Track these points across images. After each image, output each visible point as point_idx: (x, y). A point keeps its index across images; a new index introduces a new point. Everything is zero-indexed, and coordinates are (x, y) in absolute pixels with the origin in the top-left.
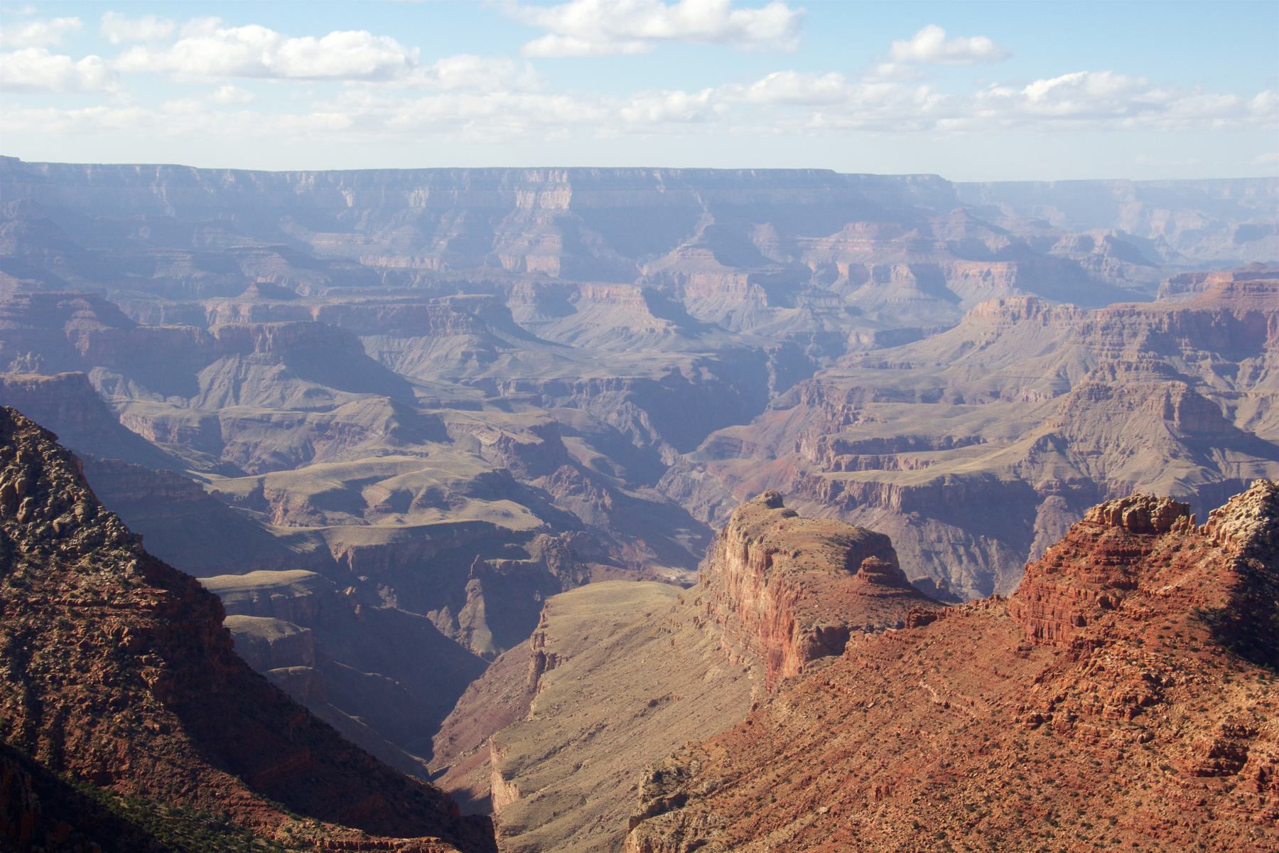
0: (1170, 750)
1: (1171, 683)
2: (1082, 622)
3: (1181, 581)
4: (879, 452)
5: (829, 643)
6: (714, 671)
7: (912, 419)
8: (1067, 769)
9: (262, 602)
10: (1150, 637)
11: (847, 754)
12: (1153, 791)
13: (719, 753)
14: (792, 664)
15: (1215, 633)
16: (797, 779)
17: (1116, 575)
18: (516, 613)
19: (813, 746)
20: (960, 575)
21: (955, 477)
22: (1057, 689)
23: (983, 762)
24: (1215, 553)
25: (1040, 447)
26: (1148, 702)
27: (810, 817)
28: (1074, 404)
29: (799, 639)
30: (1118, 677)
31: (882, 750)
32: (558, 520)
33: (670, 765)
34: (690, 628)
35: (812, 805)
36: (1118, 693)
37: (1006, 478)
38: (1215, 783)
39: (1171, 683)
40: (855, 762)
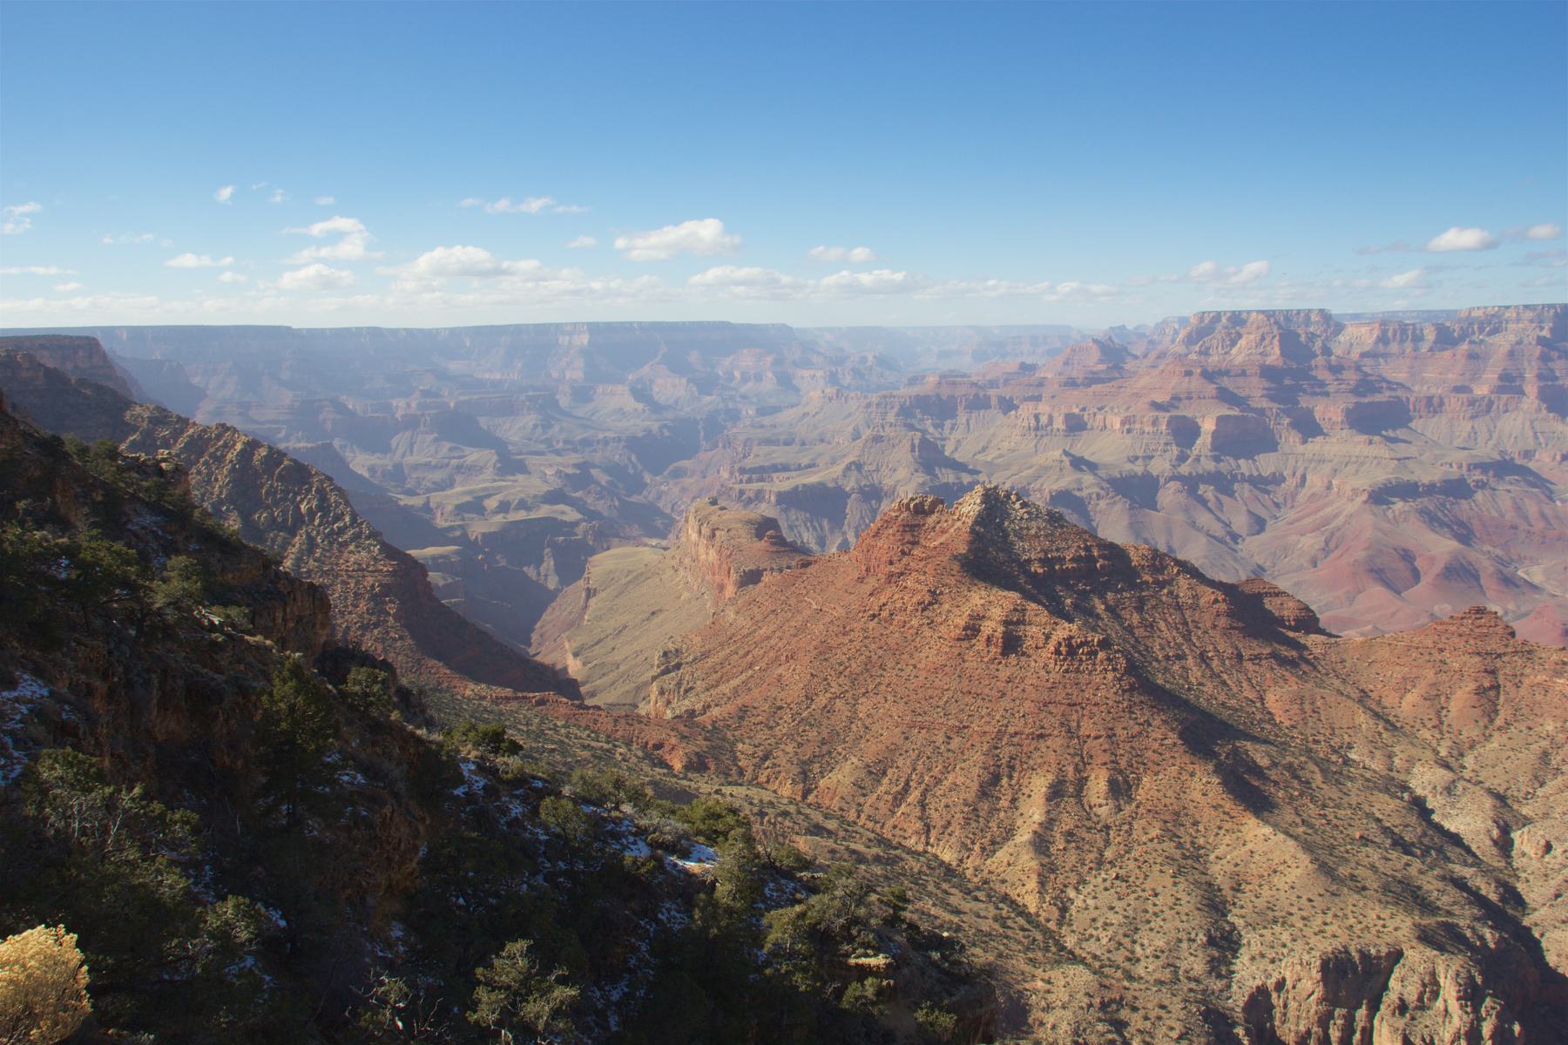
0: (943, 628)
2: (891, 563)
3: (942, 539)
4: (763, 472)
5: (751, 578)
6: (686, 595)
7: (780, 455)
8: (890, 641)
10: (930, 569)
11: (768, 638)
12: (934, 649)
14: (730, 590)
15: (962, 566)
16: (741, 652)
17: (908, 537)
18: (572, 564)
20: (808, 538)
22: (883, 600)
24: (959, 524)
25: (848, 468)
26: (930, 604)
29: (734, 576)
30: (915, 592)
32: (592, 515)
33: (671, 646)
34: (671, 572)
35: (751, 666)
36: (914, 600)
37: (831, 485)
38: (965, 644)
40: (772, 642)
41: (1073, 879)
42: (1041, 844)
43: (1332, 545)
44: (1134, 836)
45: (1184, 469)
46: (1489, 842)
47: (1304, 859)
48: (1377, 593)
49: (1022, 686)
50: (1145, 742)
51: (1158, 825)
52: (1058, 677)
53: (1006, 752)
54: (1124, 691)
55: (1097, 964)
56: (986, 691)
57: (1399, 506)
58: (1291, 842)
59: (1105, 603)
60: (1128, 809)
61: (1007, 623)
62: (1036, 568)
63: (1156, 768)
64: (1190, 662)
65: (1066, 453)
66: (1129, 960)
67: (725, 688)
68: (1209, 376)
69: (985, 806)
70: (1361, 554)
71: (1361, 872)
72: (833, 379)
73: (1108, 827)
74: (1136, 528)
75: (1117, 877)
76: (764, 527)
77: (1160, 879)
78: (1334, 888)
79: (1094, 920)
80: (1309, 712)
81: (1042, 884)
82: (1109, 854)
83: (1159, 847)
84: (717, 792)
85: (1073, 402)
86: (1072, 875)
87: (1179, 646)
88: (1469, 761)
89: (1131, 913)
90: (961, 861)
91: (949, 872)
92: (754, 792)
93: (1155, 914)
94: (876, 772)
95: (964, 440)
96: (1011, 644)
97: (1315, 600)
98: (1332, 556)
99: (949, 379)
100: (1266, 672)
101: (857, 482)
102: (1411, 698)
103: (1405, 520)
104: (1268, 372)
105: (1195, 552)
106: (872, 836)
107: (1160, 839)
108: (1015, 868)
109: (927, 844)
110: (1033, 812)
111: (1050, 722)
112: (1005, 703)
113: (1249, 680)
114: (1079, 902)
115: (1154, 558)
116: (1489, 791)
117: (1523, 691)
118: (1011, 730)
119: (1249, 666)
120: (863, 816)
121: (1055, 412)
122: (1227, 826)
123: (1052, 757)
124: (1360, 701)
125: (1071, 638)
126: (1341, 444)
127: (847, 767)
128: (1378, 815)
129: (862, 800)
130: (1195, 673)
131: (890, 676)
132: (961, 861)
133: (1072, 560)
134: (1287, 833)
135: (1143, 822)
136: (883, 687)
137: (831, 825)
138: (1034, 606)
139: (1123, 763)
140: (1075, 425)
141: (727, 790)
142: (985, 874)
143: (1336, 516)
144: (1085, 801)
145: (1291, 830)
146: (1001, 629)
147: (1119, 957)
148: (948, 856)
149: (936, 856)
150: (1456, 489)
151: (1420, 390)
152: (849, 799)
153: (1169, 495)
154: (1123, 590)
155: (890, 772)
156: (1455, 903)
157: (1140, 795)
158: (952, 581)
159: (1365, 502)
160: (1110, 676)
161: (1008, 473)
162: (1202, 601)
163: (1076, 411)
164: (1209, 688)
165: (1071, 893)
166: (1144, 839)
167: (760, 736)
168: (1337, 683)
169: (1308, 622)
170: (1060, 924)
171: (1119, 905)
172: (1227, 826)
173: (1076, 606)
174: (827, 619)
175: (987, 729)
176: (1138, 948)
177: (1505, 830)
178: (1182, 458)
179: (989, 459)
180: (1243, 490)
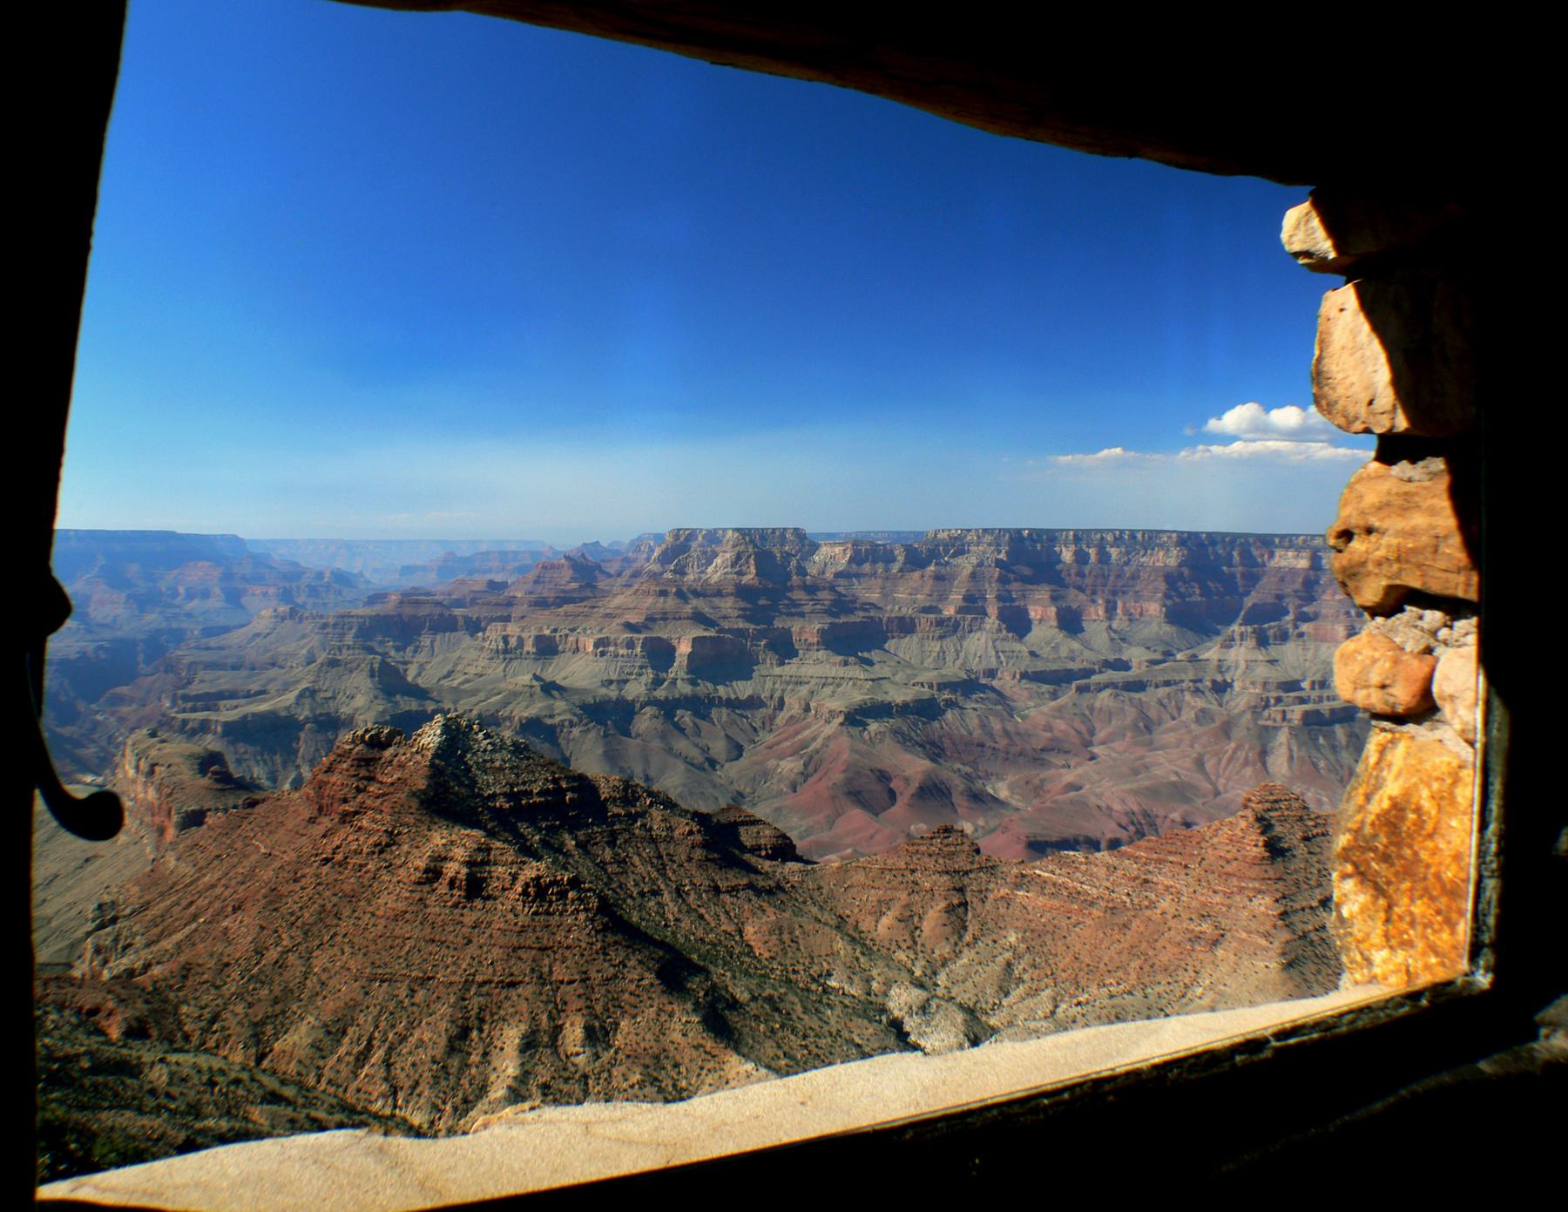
0: (401, 871)
1: (399, 833)
2: (345, 801)
4: (210, 701)
5: (194, 819)
7: (225, 680)
8: (345, 886)
10: (386, 808)
11: (213, 886)
12: (392, 895)
13: (136, 889)
14: (171, 833)
15: (422, 803)
16: (184, 903)
17: (363, 773)
19: (191, 883)
20: (259, 772)
21: (254, 714)
23: (297, 887)
25: (301, 695)
27: (194, 926)
28: (320, 670)
29: (175, 818)
30: (370, 833)
31: (233, 882)
33: (107, 898)
35: (195, 917)
36: (371, 841)
37: (284, 714)
38: (427, 888)
39: (399, 833)
40: (218, 890)
43: (811, 769)
44: (614, 1083)
45: (661, 693)
48: (856, 816)
49: (488, 932)
50: (622, 984)
51: (638, 1070)
52: (527, 920)
53: (475, 1003)
54: (597, 932)
56: (451, 938)
57: (874, 726)
59: (575, 838)
60: (606, 1056)
61: (470, 864)
62: (500, 803)
63: (634, 1011)
64: (666, 897)
65: (536, 677)
67: (167, 944)
69: (455, 1062)
70: (838, 777)
72: (286, 596)
73: (586, 1076)
74: (612, 757)
76: (208, 762)
80: (788, 942)
84: (162, 1060)
85: (544, 623)
87: (654, 881)
88: (942, 979)
90: (432, 1122)
92: (203, 1061)
94: (336, 1031)
95: (429, 665)
96: (475, 887)
97: (796, 828)
98: (810, 780)
99: (411, 598)
100: (743, 904)
101: (312, 710)
102: (885, 921)
104: (742, 592)
105: (672, 782)
106: (334, 1101)
107: (641, 1084)
109: (395, 1107)
111: (521, 968)
112: (472, 950)
113: (727, 913)
115: (625, 789)
116: (960, 1006)
117: (988, 905)
118: (479, 978)
119: (727, 898)
121: (524, 631)
123: (524, 1006)
124: (838, 928)
125: (538, 878)
126: (816, 665)
127: (303, 1028)
128: (857, 1040)
129: (321, 1063)
130: (672, 909)
131: (345, 926)
132: (432, 1122)
133: (540, 794)
134: (768, 1067)
136: (339, 939)
137: (289, 1092)
138: (499, 844)
139: (599, 1008)
140: (547, 648)
141: (173, 1058)
143: (814, 739)
144: (561, 1050)
145: (773, 1064)
146: (465, 870)
150: (926, 709)
151: (891, 611)
152: (308, 1062)
153: (645, 722)
154: (593, 824)
155: (350, 1030)
157: (619, 1040)
158: (410, 819)
159: (842, 724)
160: (582, 916)
161: (473, 700)
162: (677, 833)
163: (547, 632)
164: (686, 924)
166: (625, 1085)
167: (205, 999)
168: (815, 910)
169: (784, 850)
172: (711, 1065)
173: (544, 842)
174: (277, 864)
175: (453, 978)
178: (658, 682)
179: (455, 683)
180: (720, 715)
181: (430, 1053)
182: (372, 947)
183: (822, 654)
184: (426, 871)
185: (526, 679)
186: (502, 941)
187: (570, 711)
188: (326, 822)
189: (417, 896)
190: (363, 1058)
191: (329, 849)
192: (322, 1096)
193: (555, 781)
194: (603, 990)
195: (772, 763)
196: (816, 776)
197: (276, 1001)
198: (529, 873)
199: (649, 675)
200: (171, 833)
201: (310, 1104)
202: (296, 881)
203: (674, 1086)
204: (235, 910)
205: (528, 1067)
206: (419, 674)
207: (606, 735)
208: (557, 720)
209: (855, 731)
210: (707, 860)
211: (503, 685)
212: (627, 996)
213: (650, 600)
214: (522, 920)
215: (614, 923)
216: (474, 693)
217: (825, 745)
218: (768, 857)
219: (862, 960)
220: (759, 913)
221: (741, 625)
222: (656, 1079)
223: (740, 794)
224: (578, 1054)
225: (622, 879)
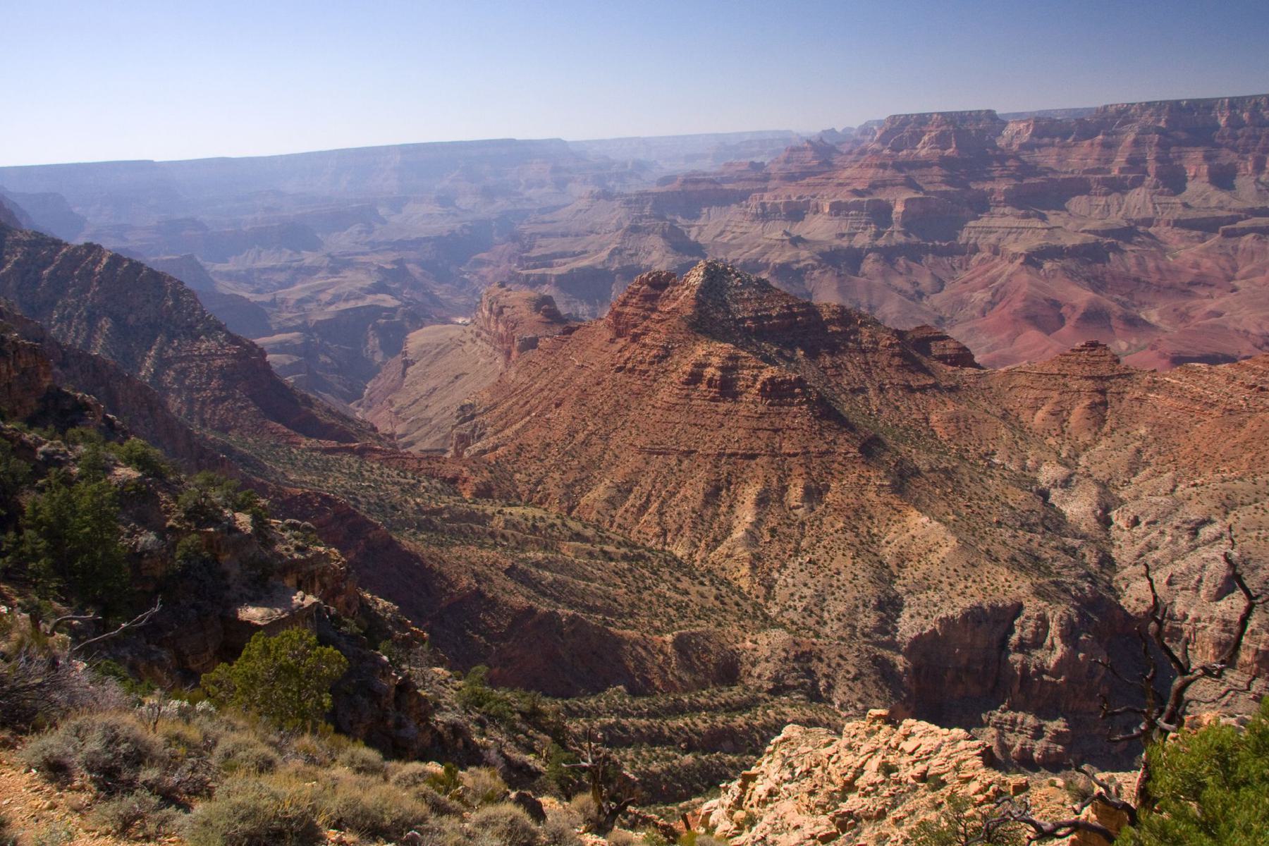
2: (635, 326)
3: (674, 305)
4: (546, 261)
5: (531, 344)
7: (556, 245)
9: (282, 348)
11: (542, 390)
12: (666, 393)
13: (487, 395)
16: (521, 403)
17: (648, 305)
18: (393, 340)
22: (627, 354)
24: (687, 292)
25: (612, 254)
29: (517, 344)
30: (652, 347)
33: (467, 402)
34: (469, 344)
35: (529, 413)
37: (600, 267)
40: (546, 393)
41: (777, 564)
42: (752, 538)
43: (997, 298)
45: (881, 242)
46: (1094, 520)
47: (953, 541)
48: (1032, 336)
49: (735, 418)
51: (841, 519)
53: (725, 469)
55: (795, 627)
56: (708, 422)
57: (1047, 265)
58: (942, 528)
60: (819, 509)
63: (841, 477)
64: (871, 393)
65: (786, 233)
66: (818, 623)
67: (508, 432)
68: (899, 166)
69: (709, 512)
70: (1018, 305)
71: (996, 547)
73: (803, 524)
75: (810, 562)
77: (842, 561)
78: (973, 560)
79: (792, 595)
81: (753, 567)
82: (804, 544)
83: (842, 537)
84: (499, 512)
85: (792, 192)
86: (775, 562)
87: (863, 382)
88: (1083, 461)
89: (820, 588)
90: (690, 555)
91: (679, 564)
92: (530, 512)
93: (839, 587)
94: (624, 490)
98: (997, 307)
102: (1040, 414)
103: (1054, 277)
104: (945, 162)
106: (621, 539)
107: (844, 530)
108: (733, 559)
109: (665, 543)
110: (746, 514)
111: (758, 444)
112: (724, 431)
114: (780, 582)
116: (1096, 481)
117: (1124, 403)
118: (728, 451)
119: (918, 395)
120: (615, 525)
122: (895, 518)
123: (760, 472)
124: (1004, 417)
126: (1002, 220)
127: (601, 488)
128: (1011, 503)
130: (875, 402)
132: (690, 555)
133: (778, 317)
134: (939, 520)
135: (831, 518)
137: (589, 532)
138: (744, 354)
140: (796, 213)
141: (507, 510)
142: (709, 565)
143: (1000, 276)
147: (810, 622)
148: (680, 552)
149: (671, 553)
152: (603, 512)
153: (868, 265)
156: (1065, 567)
157: (829, 498)
158: (681, 337)
161: (740, 251)
163: (794, 199)
165: (776, 575)
169: (963, 358)
170: (766, 600)
171: (811, 582)
172: (895, 518)
173: (780, 354)
175: (709, 452)
176: (826, 614)
177: (1107, 509)
178: (878, 235)
179: (725, 240)
181: (691, 505)
182: (652, 430)
183: (1007, 210)
184: (691, 374)
185: (777, 234)
186: (746, 424)
187: (812, 258)
188: (621, 342)
189: (684, 392)
190: (643, 509)
191: (622, 360)
192: (613, 536)
193: (789, 307)
194: (818, 461)
195: (966, 295)
196: (1001, 304)
197: (583, 469)
198: (766, 374)
199: (872, 229)
200: (515, 353)
201: (604, 540)
202: (598, 384)
203: (868, 532)
204: (557, 406)
205: (761, 516)
206: (699, 234)
207: (839, 275)
208: (802, 264)
209: (1033, 269)
210: (903, 366)
211: (761, 240)
212: (836, 465)
213: (871, 172)
214: (761, 409)
215: (827, 412)
216: (740, 246)
217: (1009, 280)
218: (952, 364)
219: (1020, 443)
220: (942, 406)
221: (944, 188)
222: (855, 527)
223: (942, 318)
224: (798, 507)
225: (838, 379)
